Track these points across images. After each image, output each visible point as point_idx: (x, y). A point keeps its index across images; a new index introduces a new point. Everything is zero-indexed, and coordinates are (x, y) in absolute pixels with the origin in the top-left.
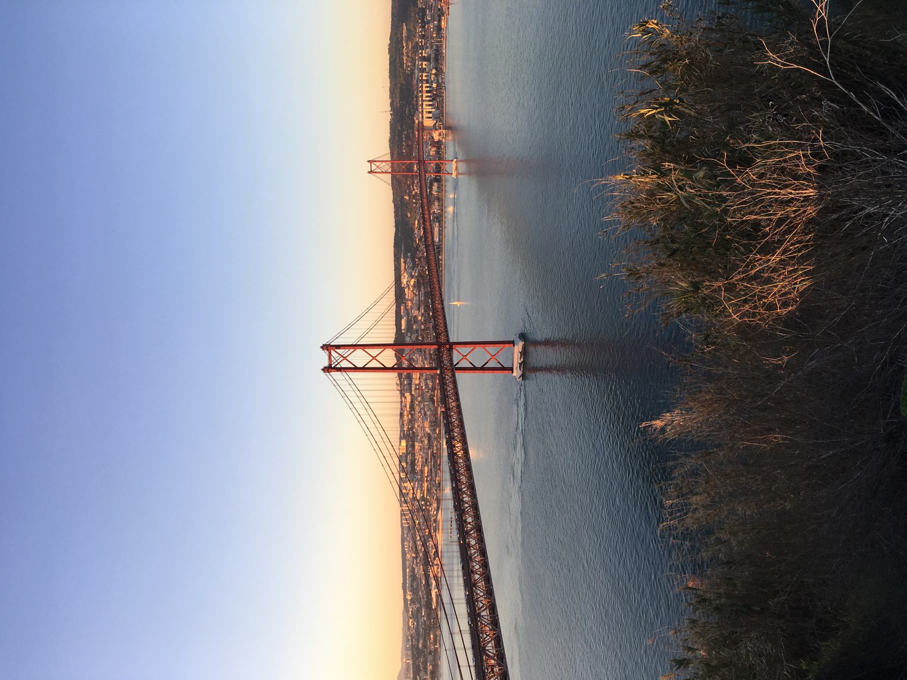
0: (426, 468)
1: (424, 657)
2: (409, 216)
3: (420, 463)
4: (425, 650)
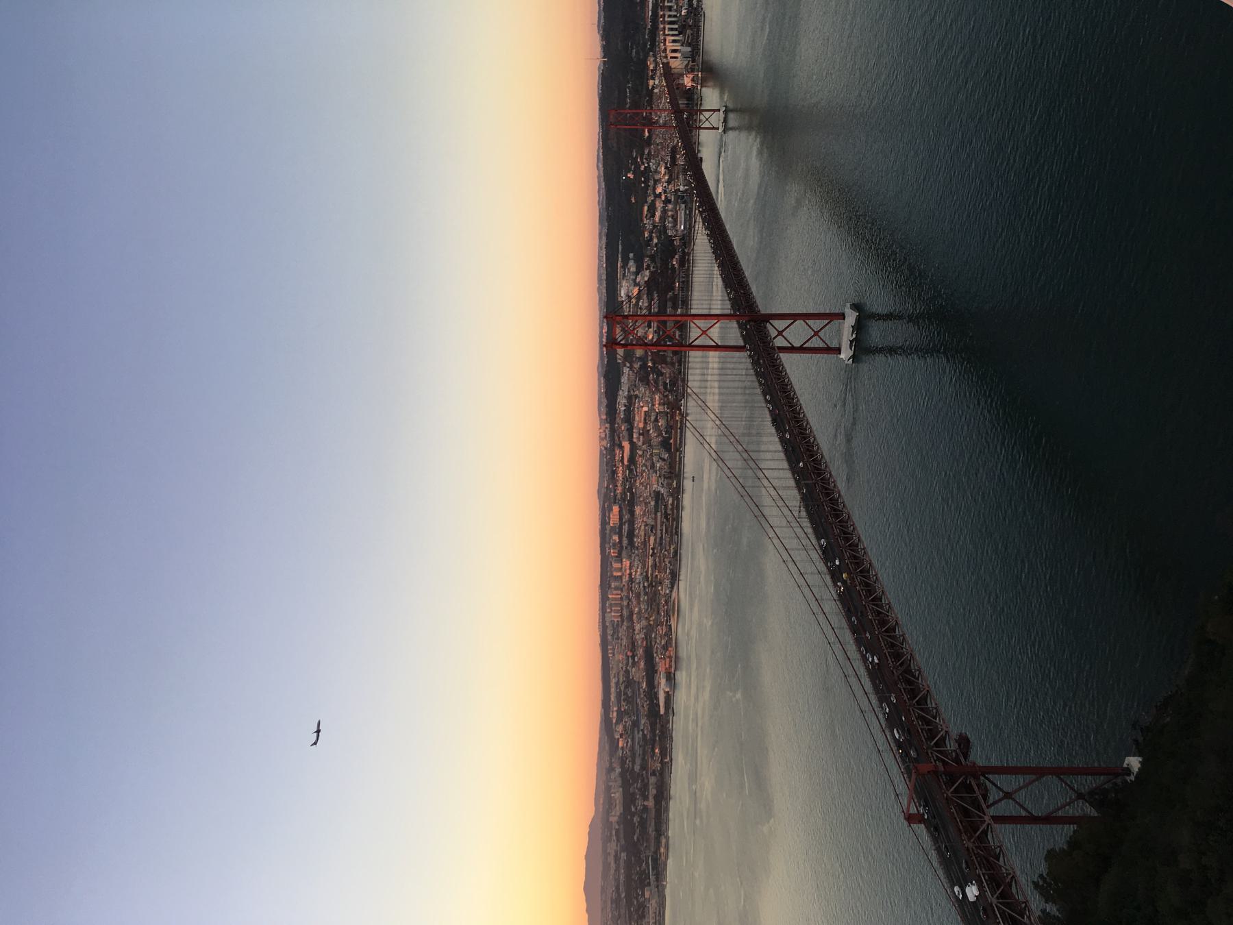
0: (652, 538)
1: (643, 781)
2: (634, 201)
3: (642, 533)
4: (644, 772)
